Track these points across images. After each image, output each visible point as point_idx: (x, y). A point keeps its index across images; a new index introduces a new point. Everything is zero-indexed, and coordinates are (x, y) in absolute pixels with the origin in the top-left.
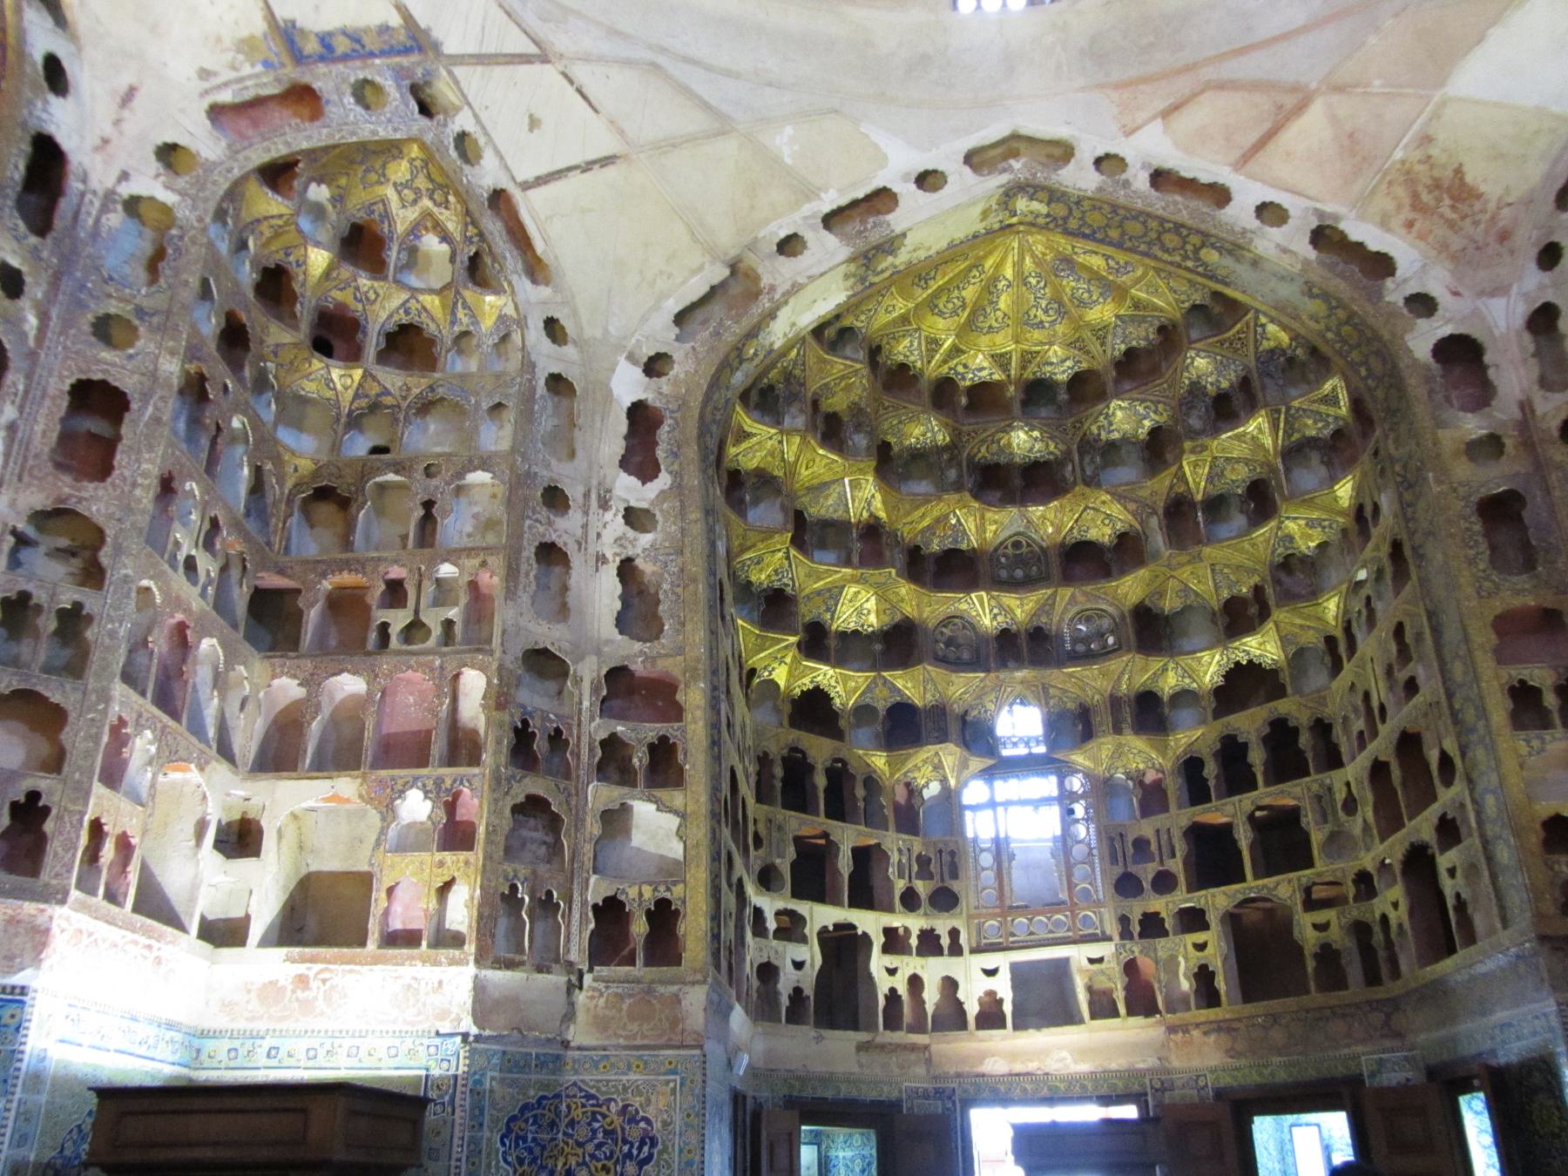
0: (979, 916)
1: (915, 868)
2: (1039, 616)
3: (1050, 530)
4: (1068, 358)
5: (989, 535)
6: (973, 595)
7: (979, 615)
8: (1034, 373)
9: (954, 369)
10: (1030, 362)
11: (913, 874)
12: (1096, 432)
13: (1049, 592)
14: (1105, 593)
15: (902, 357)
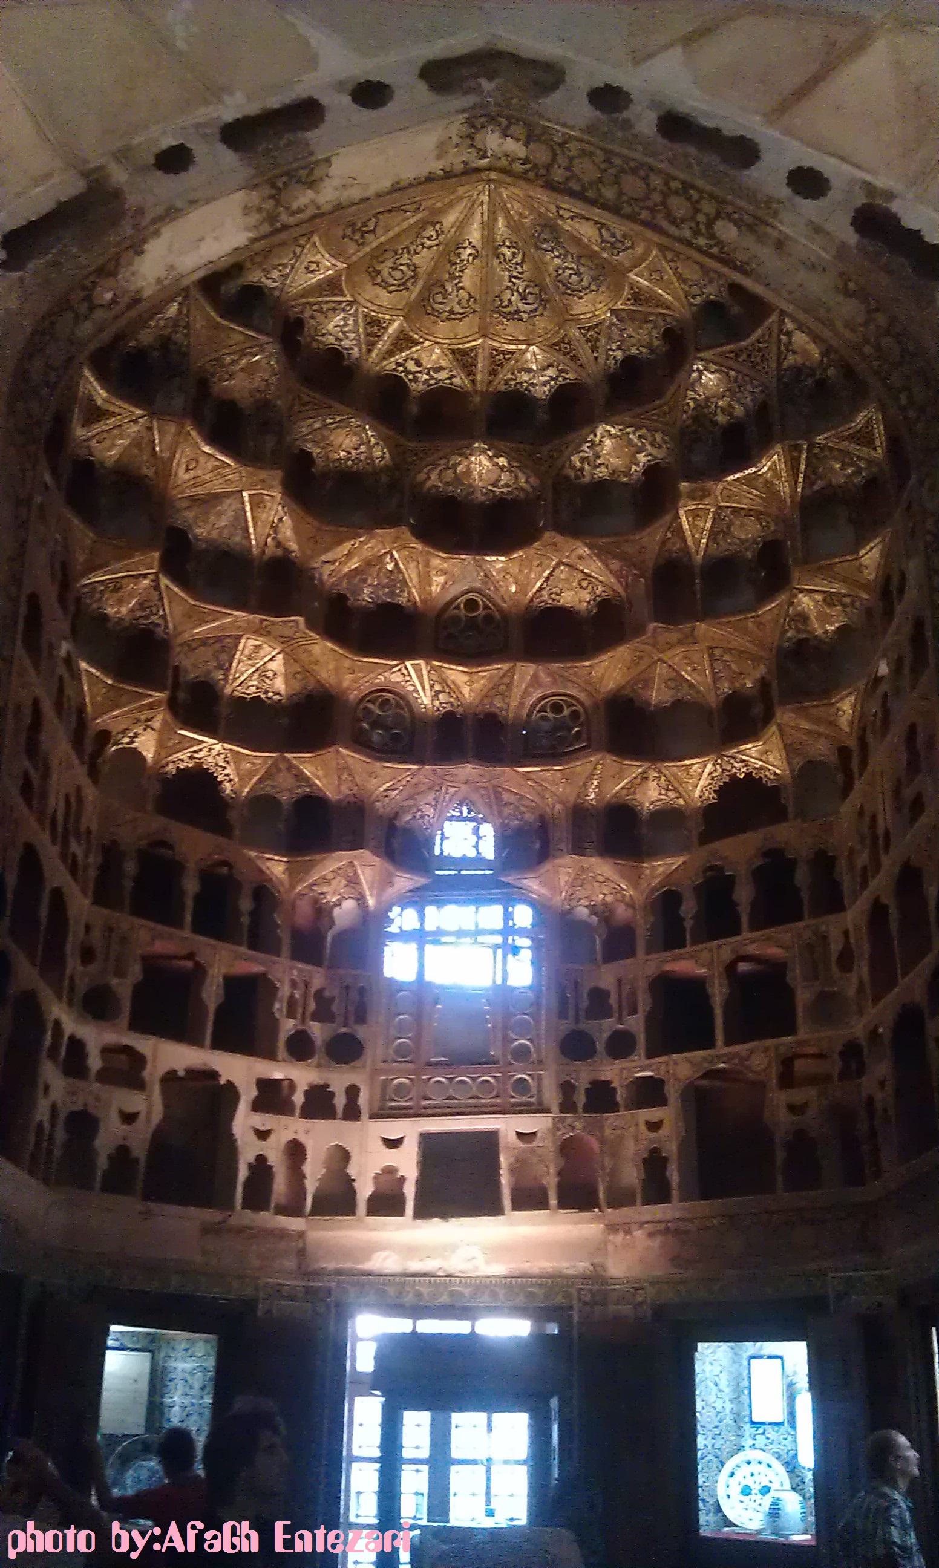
0: (386, 1072)
1: (312, 1006)
2: (492, 697)
3: (513, 589)
4: (550, 365)
5: (435, 589)
6: (408, 664)
7: (416, 691)
8: (507, 382)
10: (501, 365)
11: (308, 1014)
12: (578, 464)
13: (506, 666)
14: (575, 674)
15: (332, 340)
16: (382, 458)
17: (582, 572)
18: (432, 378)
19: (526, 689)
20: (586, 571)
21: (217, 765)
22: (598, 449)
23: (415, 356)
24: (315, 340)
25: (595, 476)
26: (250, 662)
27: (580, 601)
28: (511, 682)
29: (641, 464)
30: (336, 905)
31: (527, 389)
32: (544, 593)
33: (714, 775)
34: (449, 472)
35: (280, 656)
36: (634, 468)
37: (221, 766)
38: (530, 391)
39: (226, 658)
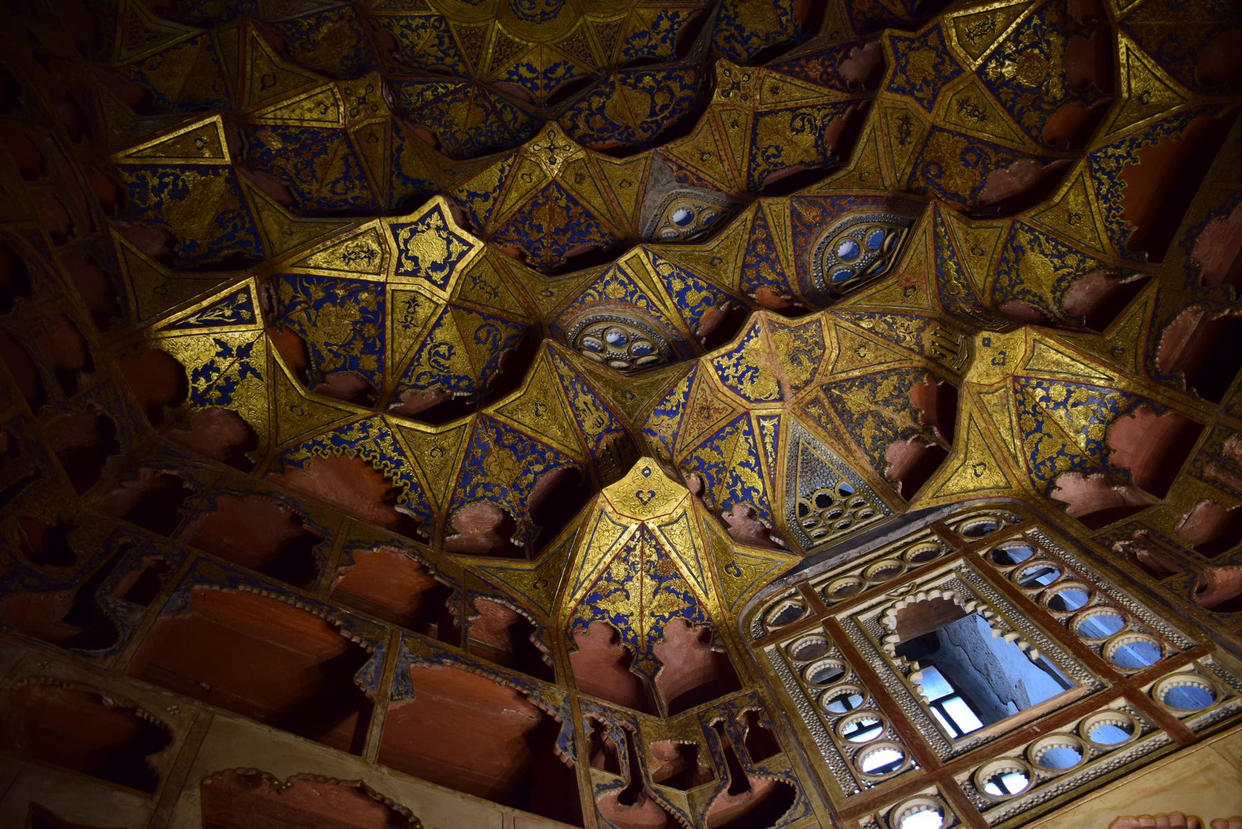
4: (660, 18)
5: (629, 207)
6: (622, 261)
7: (650, 305)
9: (516, 73)
12: (727, 46)
13: (748, 215)
15: (432, 60)
16: (515, 119)
17: (787, 110)
18: (551, 80)
19: (794, 242)
20: (791, 104)
21: (383, 456)
22: (738, 21)
23: (525, 61)
24: (416, 61)
25: (751, 51)
26: (409, 332)
27: (807, 151)
28: (769, 235)
29: (788, 9)
30: (652, 639)
31: (649, 53)
32: (759, 160)
33: (1104, 190)
34: (598, 117)
35: (448, 317)
36: (784, 19)
37: (391, 459)
38: (654, 54)
39: (373, 331)
